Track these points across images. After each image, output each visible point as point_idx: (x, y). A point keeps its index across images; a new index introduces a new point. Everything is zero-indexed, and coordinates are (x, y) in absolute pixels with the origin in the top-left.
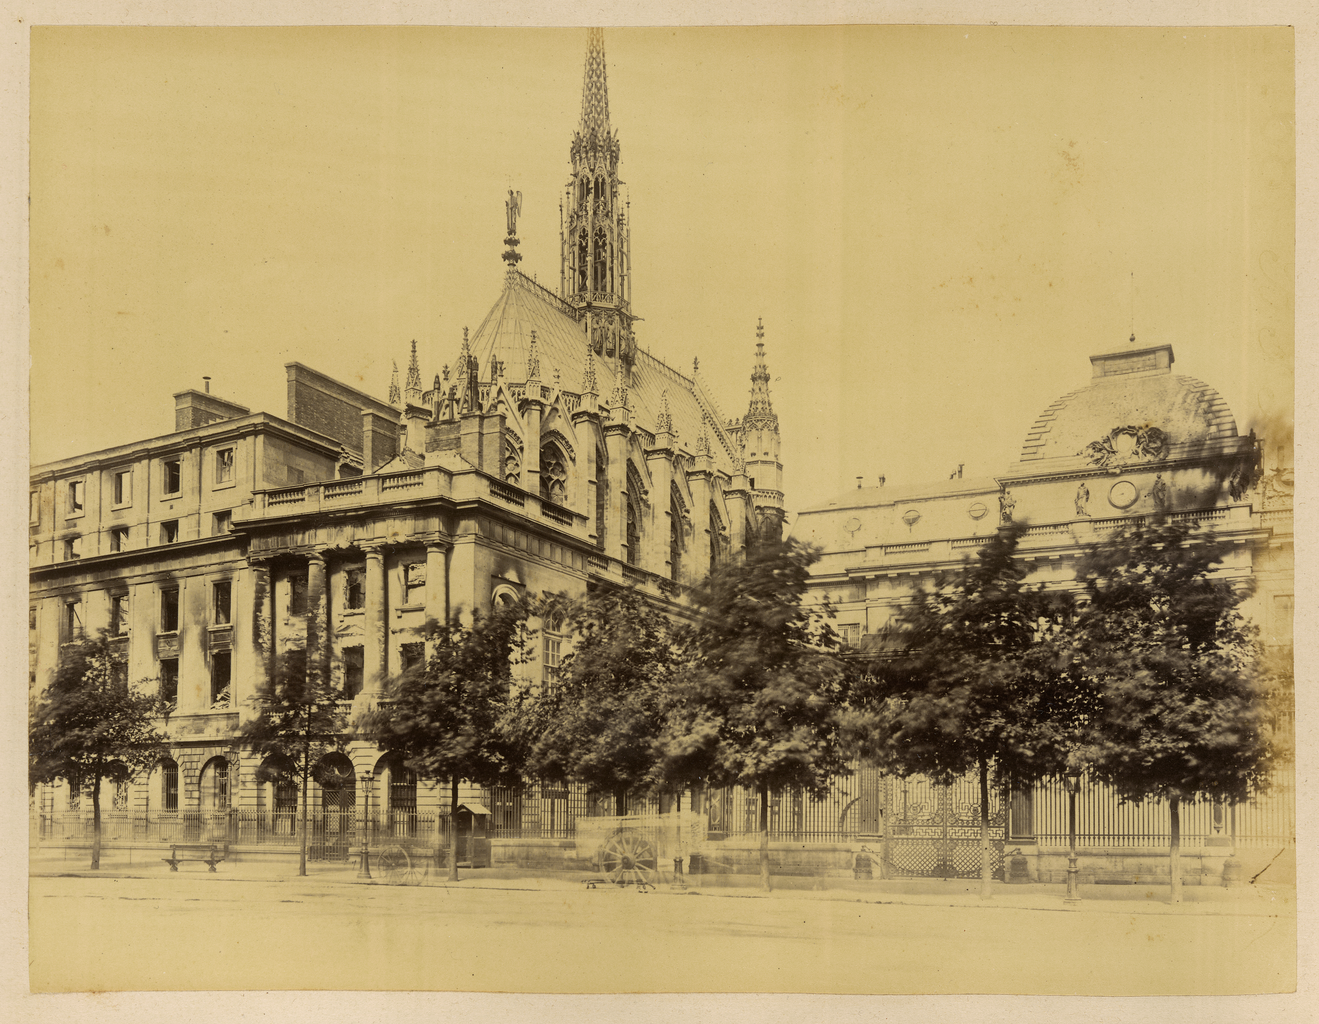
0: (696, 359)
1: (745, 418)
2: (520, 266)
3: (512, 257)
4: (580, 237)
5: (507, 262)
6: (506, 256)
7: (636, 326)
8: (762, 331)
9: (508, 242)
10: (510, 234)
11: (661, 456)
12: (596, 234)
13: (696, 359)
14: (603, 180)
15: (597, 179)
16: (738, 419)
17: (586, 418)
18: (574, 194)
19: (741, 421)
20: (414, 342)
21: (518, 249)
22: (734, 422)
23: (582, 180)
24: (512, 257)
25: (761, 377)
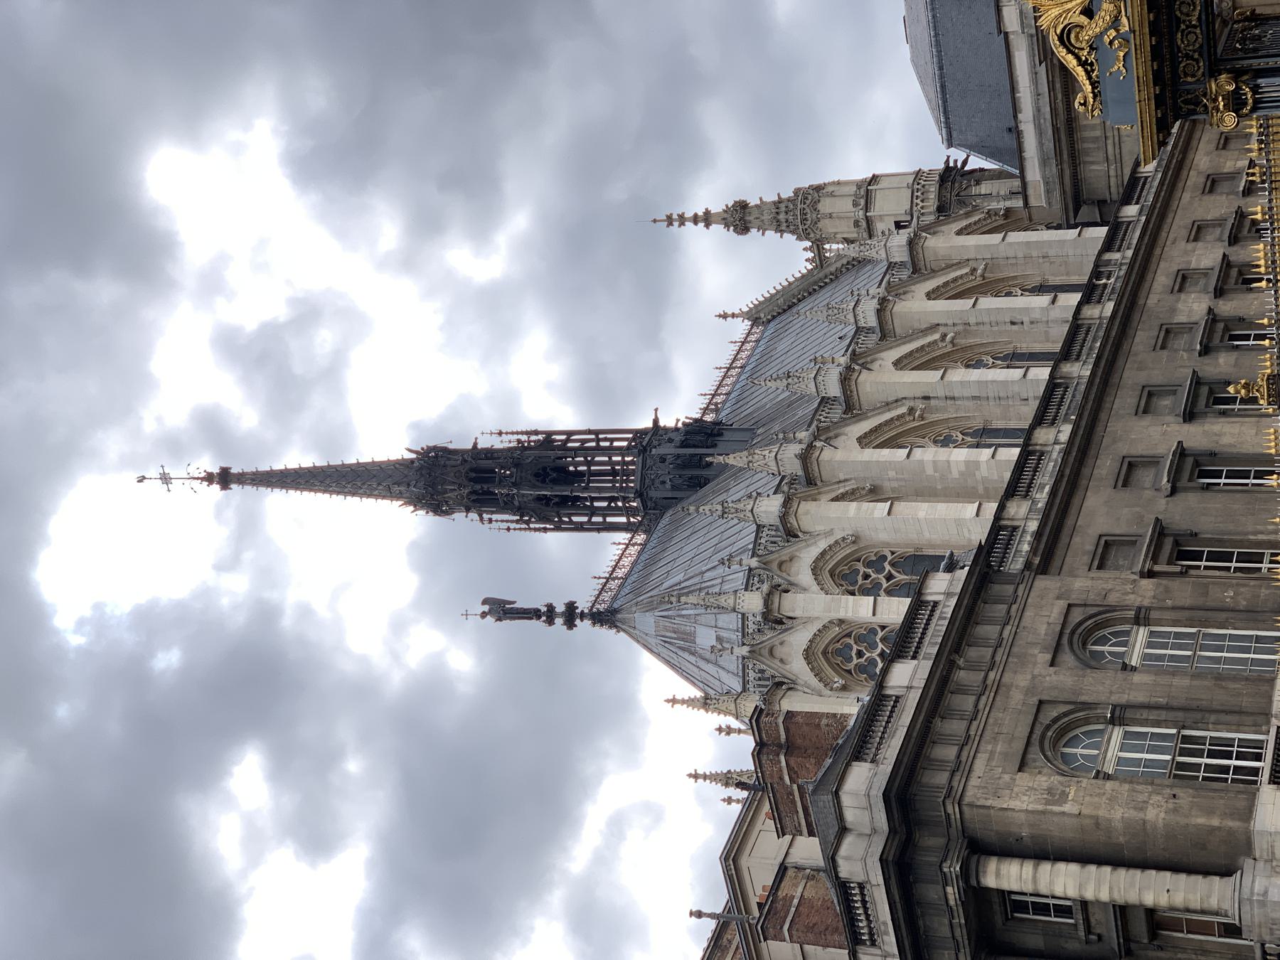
0: (720, 316)
1: (799, 238)
2: (583, 605)
3: (571, 615)
4: (547, 505)
5: (578, 622)
6: (570, 624)
7: (667, 421)
8: (675, 216)
9: (550, 621)
10: (539, 617)
11: (853, 387)
12: (543, 481)
13: (720, 316)
14: (472, 470)
15: (471, 480)
16: (805, 249)
17: (792, 520)
18: (492, 513)
19: (808, 244)
20: (695, 776)
21: (560, 608)
22: (810, 255)
23: (474, 501)
24: (571, 615)
25: (740, 218)
